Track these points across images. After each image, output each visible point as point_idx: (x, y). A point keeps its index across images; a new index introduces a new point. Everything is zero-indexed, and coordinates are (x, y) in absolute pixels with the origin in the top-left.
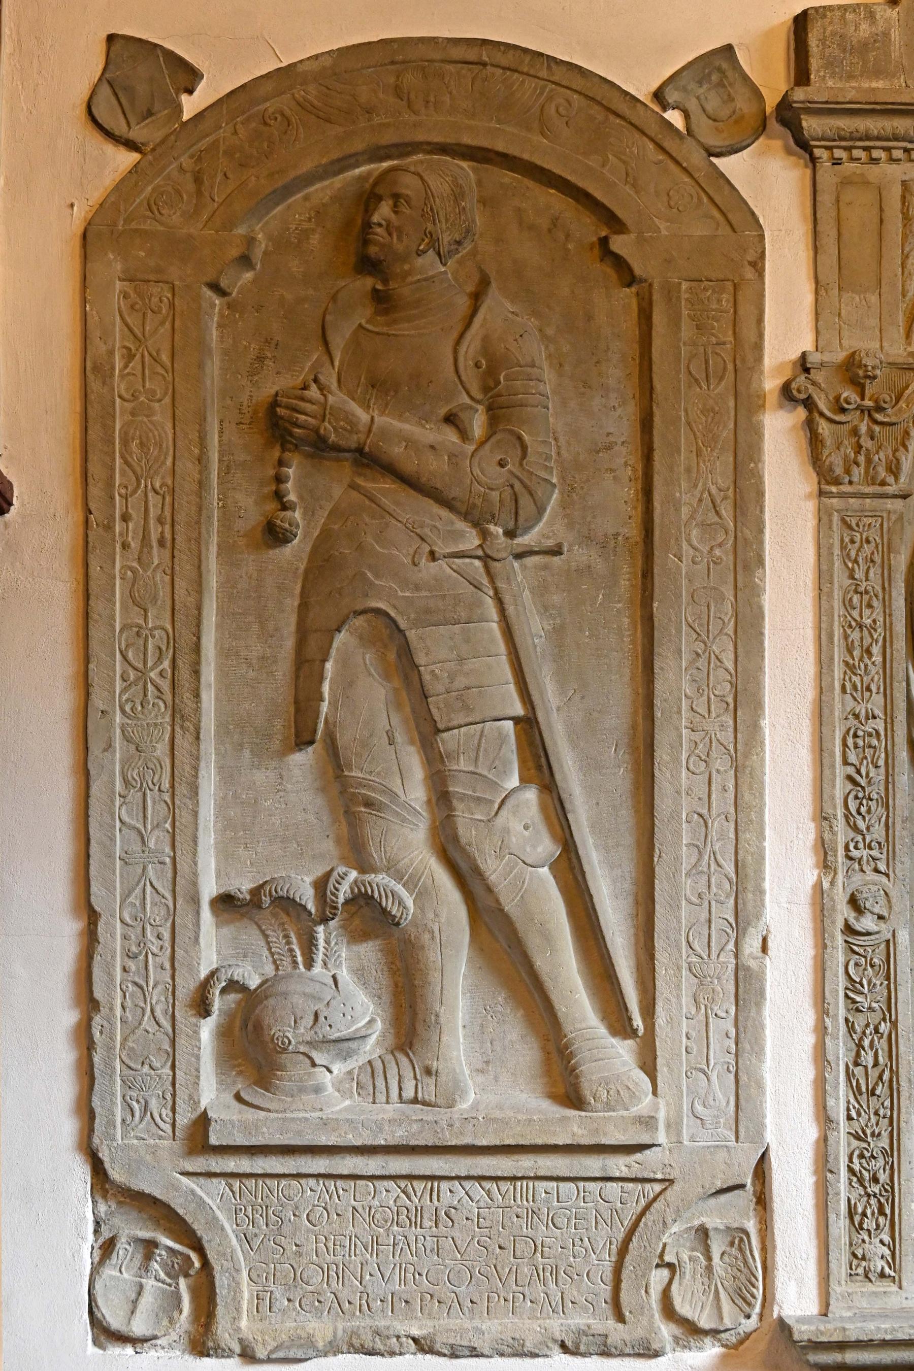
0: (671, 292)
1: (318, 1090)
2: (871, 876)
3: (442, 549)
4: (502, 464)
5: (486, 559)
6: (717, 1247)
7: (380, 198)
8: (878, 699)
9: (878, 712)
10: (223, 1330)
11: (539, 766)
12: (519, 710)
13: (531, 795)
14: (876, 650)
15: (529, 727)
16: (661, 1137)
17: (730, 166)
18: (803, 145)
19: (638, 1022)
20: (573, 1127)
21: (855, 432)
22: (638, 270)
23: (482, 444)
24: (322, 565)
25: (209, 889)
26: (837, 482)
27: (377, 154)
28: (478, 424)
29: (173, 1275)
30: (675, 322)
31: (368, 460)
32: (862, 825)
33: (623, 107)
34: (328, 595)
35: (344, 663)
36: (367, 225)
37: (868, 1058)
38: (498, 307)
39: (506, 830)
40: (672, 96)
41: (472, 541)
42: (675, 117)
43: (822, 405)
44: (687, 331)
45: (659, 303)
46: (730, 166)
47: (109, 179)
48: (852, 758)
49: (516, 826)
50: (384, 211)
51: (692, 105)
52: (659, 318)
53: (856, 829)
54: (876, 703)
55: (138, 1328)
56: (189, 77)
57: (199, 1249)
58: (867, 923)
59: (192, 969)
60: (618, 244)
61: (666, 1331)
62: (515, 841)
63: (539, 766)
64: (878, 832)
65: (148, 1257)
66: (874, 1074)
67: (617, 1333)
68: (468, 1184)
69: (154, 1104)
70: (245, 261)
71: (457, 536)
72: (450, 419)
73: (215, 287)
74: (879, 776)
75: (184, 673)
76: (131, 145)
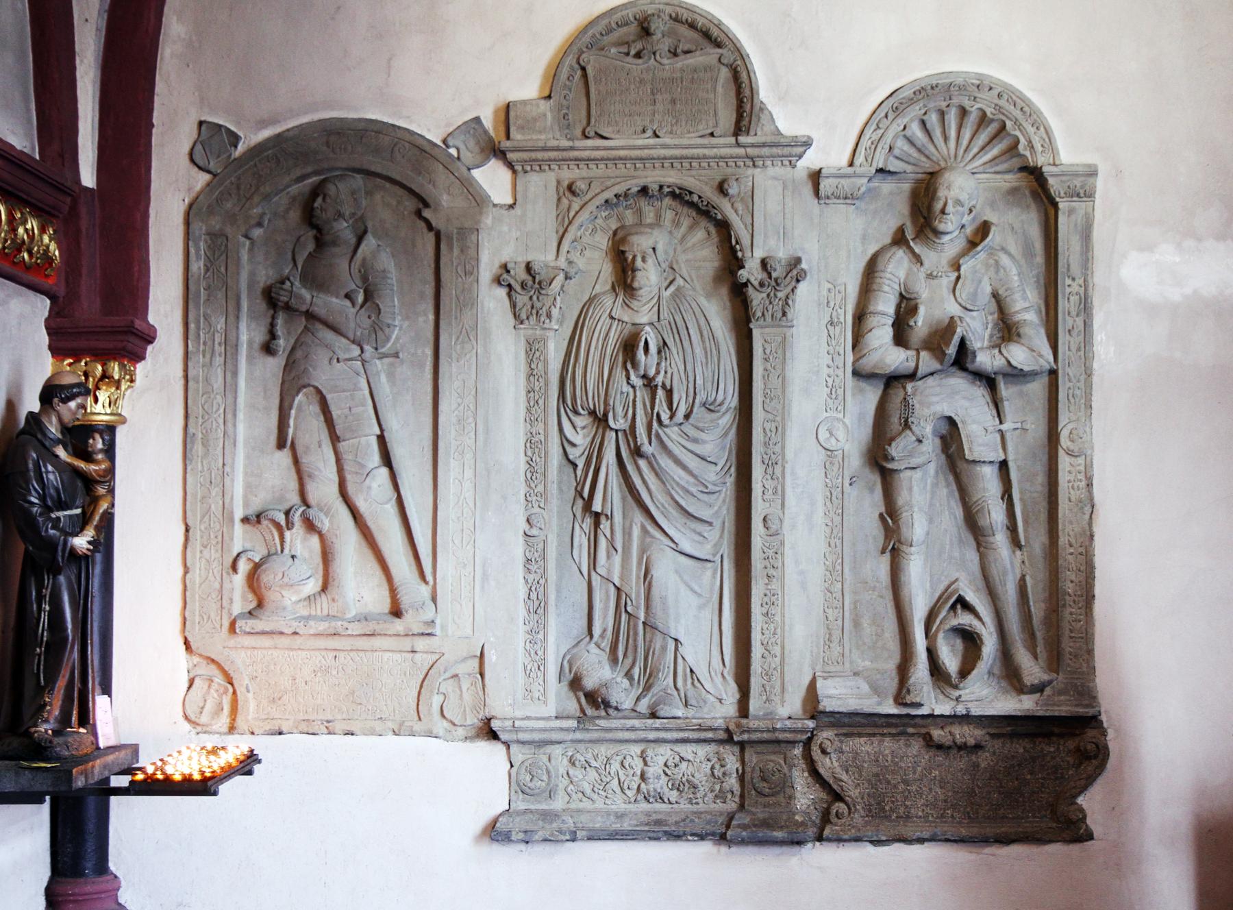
0: (450, 238)
1: (284, 608)
2: (536, 510)
3: (342, 356)
4: (369, 317)
5: (363, 362)
6: (465, 686)
7: (318, 195)
8: (541, 425)
9: (542, 432)
10: (240, 722)
11: (387, 460)
12: (378, 432)
13: (384, 471)
14: (541, 402)
15: (382, 439)
16: (437, 631)
17: (476, 173)
18: (510, 165)
19: (429, 578)
20: (398, 625)
21: (531, 298)
22: (434, 224)
23: (362, 307)
24: (289, 366)
25: (239, 514)
26: (522, 323)
27: (316, 173)
28: (360, 298)
29: (221, 696)
30: (451, 248)
31: (310, 316)
32: (533, 485)
33: (428, 148)
34: (293, 380)
35: (299, 409)
36: (313, 209)
37: (534, 596)
38: (370, 242)
39: (369, 488)
40: (451, 142)
41: (356, 351)
42: (453, 151)
43: (518, 288)
44: (456, 251)
45: (441, 243)
46: (476, 173)
47: (198, 187)
48: (529, 453)
49: (375, 485)
50: (318, 202)
51: (462, 147)
52: (443, 246)
53: (529, 486)
54: (540, 427)
55: (204, 719)
56: (234, 139)
57: (232, 684)
58: (534, 532)
59: (230, 551)
60: (427, 213)
61: (441, 726)
62: (374, 494)
63: (387, 460)
64: (540, 488)
65: (209, 686)
66: (536, 604)
67: (417, 727)
68: (352, 654)
69: (213, 615)
70: (260, 224)
71: (349, 350)
72: (347, 296)
73: (247, 237)
74: (541, 462)
75: (229, 416)
76: (209, 172)
